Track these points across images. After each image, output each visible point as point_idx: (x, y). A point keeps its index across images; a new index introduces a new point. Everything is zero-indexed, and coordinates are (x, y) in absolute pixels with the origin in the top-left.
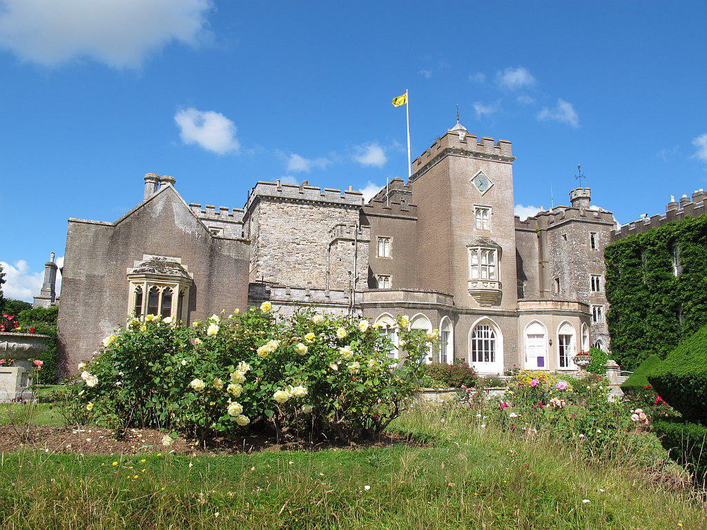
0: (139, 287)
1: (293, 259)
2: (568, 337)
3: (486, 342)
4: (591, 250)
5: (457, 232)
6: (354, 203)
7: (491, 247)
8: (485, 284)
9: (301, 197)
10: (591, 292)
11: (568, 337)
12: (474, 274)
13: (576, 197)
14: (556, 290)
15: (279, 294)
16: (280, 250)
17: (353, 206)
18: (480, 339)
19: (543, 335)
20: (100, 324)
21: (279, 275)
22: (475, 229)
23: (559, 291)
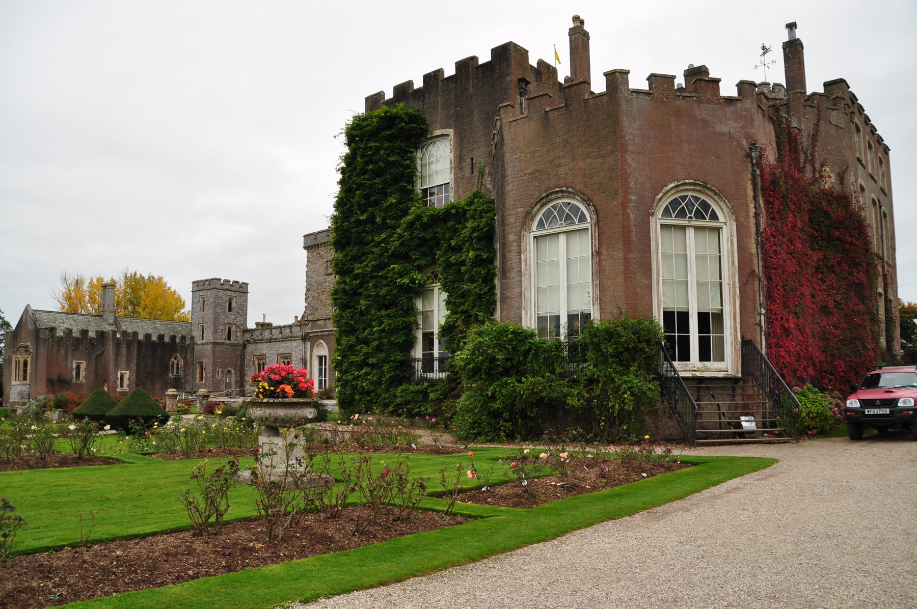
15: (267, 334)
16: (318, 291)
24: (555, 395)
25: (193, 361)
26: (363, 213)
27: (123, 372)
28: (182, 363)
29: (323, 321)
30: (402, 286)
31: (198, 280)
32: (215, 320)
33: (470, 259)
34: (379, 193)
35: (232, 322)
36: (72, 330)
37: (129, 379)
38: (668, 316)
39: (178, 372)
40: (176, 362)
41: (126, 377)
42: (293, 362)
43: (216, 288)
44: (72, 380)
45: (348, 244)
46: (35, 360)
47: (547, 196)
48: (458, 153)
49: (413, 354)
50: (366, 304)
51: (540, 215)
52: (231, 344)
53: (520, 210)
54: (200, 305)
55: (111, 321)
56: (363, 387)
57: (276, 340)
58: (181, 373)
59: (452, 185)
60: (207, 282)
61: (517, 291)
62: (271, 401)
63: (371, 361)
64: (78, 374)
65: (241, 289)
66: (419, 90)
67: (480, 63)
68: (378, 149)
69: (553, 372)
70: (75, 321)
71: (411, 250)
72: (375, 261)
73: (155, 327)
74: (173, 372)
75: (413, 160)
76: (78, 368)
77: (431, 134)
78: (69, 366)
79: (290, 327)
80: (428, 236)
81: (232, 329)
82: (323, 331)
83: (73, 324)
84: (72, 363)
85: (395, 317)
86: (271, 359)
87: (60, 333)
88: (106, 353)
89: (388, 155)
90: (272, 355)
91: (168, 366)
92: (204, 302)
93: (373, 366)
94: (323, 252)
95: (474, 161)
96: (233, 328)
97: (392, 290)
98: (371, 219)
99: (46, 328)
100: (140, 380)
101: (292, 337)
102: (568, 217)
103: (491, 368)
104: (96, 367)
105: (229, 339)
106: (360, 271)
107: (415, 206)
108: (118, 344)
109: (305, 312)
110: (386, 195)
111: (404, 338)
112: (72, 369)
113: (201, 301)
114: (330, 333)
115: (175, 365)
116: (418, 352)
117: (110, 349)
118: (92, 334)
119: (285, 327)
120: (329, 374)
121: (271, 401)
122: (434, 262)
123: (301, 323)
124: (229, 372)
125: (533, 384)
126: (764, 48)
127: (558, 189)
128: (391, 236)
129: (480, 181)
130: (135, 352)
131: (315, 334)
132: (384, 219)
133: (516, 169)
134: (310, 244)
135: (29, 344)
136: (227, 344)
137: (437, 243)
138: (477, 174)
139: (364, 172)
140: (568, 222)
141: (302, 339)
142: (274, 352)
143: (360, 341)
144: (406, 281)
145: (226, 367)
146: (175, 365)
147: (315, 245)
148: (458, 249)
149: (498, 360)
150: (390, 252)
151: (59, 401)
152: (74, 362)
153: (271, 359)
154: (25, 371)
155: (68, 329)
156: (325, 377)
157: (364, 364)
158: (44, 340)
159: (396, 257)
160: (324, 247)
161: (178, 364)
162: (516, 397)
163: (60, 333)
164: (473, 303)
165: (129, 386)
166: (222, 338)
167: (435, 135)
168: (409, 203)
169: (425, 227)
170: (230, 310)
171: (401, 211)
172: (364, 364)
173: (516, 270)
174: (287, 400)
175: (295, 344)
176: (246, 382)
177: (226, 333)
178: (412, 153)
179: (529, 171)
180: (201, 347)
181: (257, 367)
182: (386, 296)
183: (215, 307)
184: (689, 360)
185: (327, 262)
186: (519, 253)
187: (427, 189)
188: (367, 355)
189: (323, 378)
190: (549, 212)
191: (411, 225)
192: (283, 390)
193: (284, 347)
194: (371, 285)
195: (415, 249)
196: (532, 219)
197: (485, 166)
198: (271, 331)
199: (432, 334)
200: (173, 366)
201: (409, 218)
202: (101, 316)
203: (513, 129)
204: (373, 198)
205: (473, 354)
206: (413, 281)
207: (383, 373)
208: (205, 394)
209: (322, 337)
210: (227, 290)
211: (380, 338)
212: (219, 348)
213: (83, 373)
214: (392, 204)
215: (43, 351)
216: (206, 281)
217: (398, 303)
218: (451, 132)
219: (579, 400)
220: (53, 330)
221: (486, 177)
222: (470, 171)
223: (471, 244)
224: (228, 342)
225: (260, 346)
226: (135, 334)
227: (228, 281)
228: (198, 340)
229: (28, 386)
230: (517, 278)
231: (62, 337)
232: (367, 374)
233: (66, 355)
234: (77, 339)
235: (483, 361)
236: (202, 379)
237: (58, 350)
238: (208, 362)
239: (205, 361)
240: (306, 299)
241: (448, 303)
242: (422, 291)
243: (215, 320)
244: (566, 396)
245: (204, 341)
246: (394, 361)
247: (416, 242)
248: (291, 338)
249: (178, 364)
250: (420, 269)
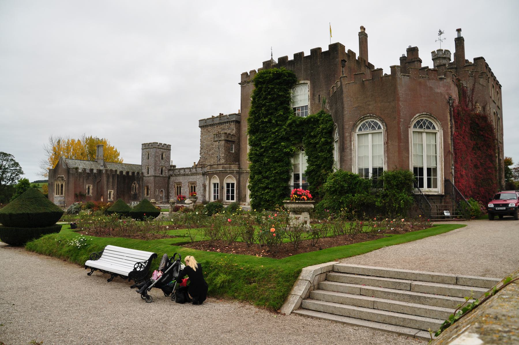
1: (211, 152)
16: (207, 150)
17: (232, 121)
21: (206, 161)
24: (370, 201)
25: (143, 185)
26: (265, 118)
27: (111, 191)
28: (137, 186)
29: (216, 166)
30: (285, 152)
31: (145, 143)
32: (155, 164)
33: (322, 142)
34: (273, 109)
35: (163, 165)
36: (86, 169)
37: (113, 194)
38: (415, 169)
39: (135, 191)
40: (134, 186)
41: (112, 193)
42: (197, 186)
43: (156, 148)
44: (86, 194)
45: (257, 132)
46: (67, 184)
47: (364, 117)
48: (312, 92)
49: (289, 183)
50: (267, 160)
51: (360, 125)
52: (163, 177)
53: (351, 123)
54: (147, 156)
55: (102, 164)
56: (266, 199)
57: (188, 175)
58: (137, 191)
59: (309, 106)
60: (151, 144)
61: (349, 157)
62: (300, 202)
63: (270, 186)
64: (89, 191)
65: (167, 148)
66: (291, 61)
67: (322, 51)
68: (272, 89)
69: (367, 192)
70: (85, 164)
71: (290, 136)
72: (272, 140)
73: (123, 168)
74: (133, 191)
75: (289, 94)
76: (89, 188)
77: (298, 82)
78: (85, 187)
79: (190, 168)
80: (299, 130)
81: (163, 169)
82: (217, 171)
83: (84, 165)
84: (86, 186)
85: (282, 166)
86: (185, 184)
87: (80, 171)
88: (102, 180)
89: (278, 92)
90: (185, 182)
91: (131, 188)
92: (149, 155)
93: (271, 189)
94: (210, 129)
95: (320, 97)
96: (164, 168)
97: (281, 154)
98: (270, 121)
99: (73, 168)
100: (119, 194)
101: (197, 173)
102: (373, 127)
103: (341, 190)
104: (97, 188)
105: (162, 174)
106: (264, 145)
107: (291, 115)
108: (108, 177)
109: (200, 160)
110: (276, 110)
111: (286, 176)
112: (86, 189)
113: (147, 154)
114: (221, 171)
115: (134, 187)
116: (292, 183)
117: (105, 179)
118: (95, 171)
119: (186, 168)
120: (220, 192)
121: (300, 202)
122: (301, 142)
123: (201, 165)
124: (162, 191)
125: (360, 197)
126: (440, 31)
127: (369, 115)
128: (280, 129)
129: (323, 106)
130: (116, 181)
131: (212, 172)
132: (276, 121)
133: (349, 105)
134: (202, 125)
135: (63, 176)
136: (161, 177)
137: (303, 133)
138: (322, 103)
139: (265, 98)
140: (373, 129)
141: (202, 174)
142: (186, 181)
143: (264, 178)
144: (288, 150)
145: (160, 188)
146: (134, 187)
147: (205, 126)
148: (315, 137)
149: (345, 187)
150: (280, 137)
151: (90, 205)
152: (87, 185)
153: (185, 184)
154: (62, 190)
155: (84, 168)
156: (218, 193)
157: (266, 188)
158: (73, 174)
159: (283, 139)
160: (211, 126)
161: (135, 187)
162: (352, 202)
163: (80, 171)
164: (322, 161)
165: (113, 198)
166: (158, 173)
167: (300, 83)
168: (288, 114)
169: (298, 126)
170: (162, 159)
171: (284, 118)
172: (266, 188)
173: (349, 148)
174: (305, 201)
175: (198, 177)
176: (170, 196)
177: (161, 171)
178: (289, 91)
179: (355, 106)
180: (148, 178)
181: (176, 188)
182: (278, 157)
183: (155, 157)
184: (423, 187)
185: (214, 135)
186: (351, 141)
187: (296, 108)
188: (268, 184)
189: (216, 195)
190: (364, 125)
191: (290, 125)
192: (303, 198)
193: (192, 179)
194: (270, 151)
195: (292, 136)
196: (357, 127)
197: (326, 99)
198: (185, 170)
199: (299, 174)
200: (133, 188)
201: (289, 122)
202: (97, 162)
203: (347, 87)
204: (270, 111)
205: (334, 184)
206: (291, 150)
207: (276, 192)
208: (174, 202)
209: (216, 174)
210: (161, 148)
211: (274, 176)
212: (157, 179)
213: (91, 191)
214: (281, 114)
215: (72, 180)
216: (150, 143)
217: (284, 160)
218: (309, 82)
219: (380, 204)
220: (77, 169)
221: (326, 104)
222: (318, 101)
223: (322, 135)
224: (161, 175)
225: (178, 178)
226: (116, 171)
227: (161, 144)
228: (146, 174)
229: (63, 198)
230: (349, 152)
231: (81, 172)
232: (268, 192)
233: (83, 182)
234: (88, 173)
235: (338, 187)
236: (148, 194)
237: (79, 179)
238: (151, 186)
239: (149, 185)
240: (200, 153)
241: (308, 161)
242: (294, 155)
243: (155, 164)
244: (375, 202)
245: (149, 175)
246: (282, 187)
247: (293, 132)
248: (196, 174)
249: (135, 187)
250: (294, 144)
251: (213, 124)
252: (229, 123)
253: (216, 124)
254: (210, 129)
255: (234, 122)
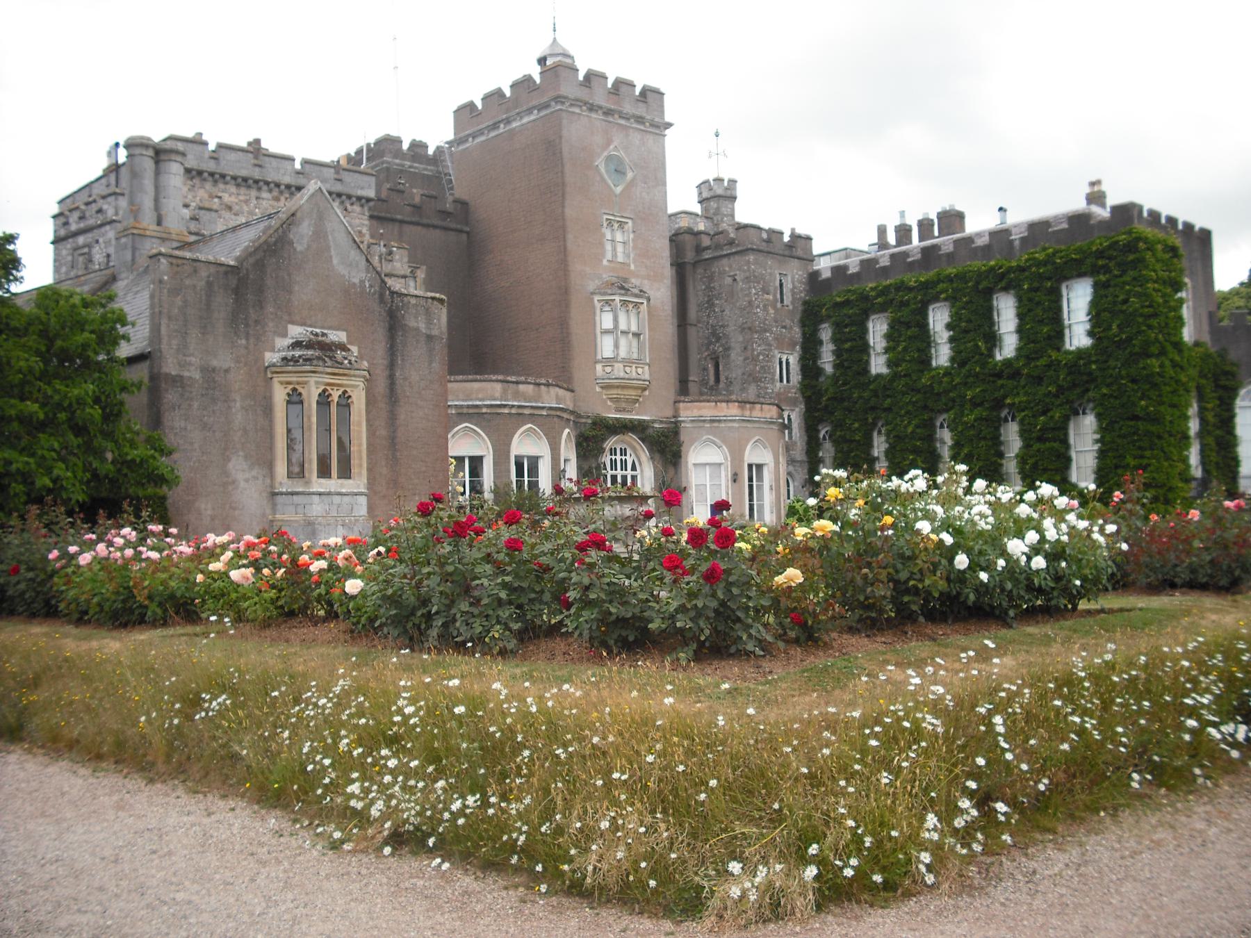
0: (294, 390)
2: (760, 467)
3: (624, 478)
4: (779, 305)
5: (576, 267)
6: (360, 193)
7: (636, 296)
8: (628, 369)
9: (256, 173)
10: (778, 384)
11: (760, 467)
12: (606, 347)
13: (711, 194)
14: (712, 378)
17: (359, 198)
18: (614, 472)
19: (720, 464)
20: (230, 465)
22: (605, 262)
23: (717, 380)
29: (531, 387)
46: (383, 405)
131: (514, 411)
147: (212, 174)
160: (238, 185)
209: (532, 418)
251: (256, 182)
252: (342, 203)
253: (278, 185)
254: (233, 199)
255: (362, 206)
